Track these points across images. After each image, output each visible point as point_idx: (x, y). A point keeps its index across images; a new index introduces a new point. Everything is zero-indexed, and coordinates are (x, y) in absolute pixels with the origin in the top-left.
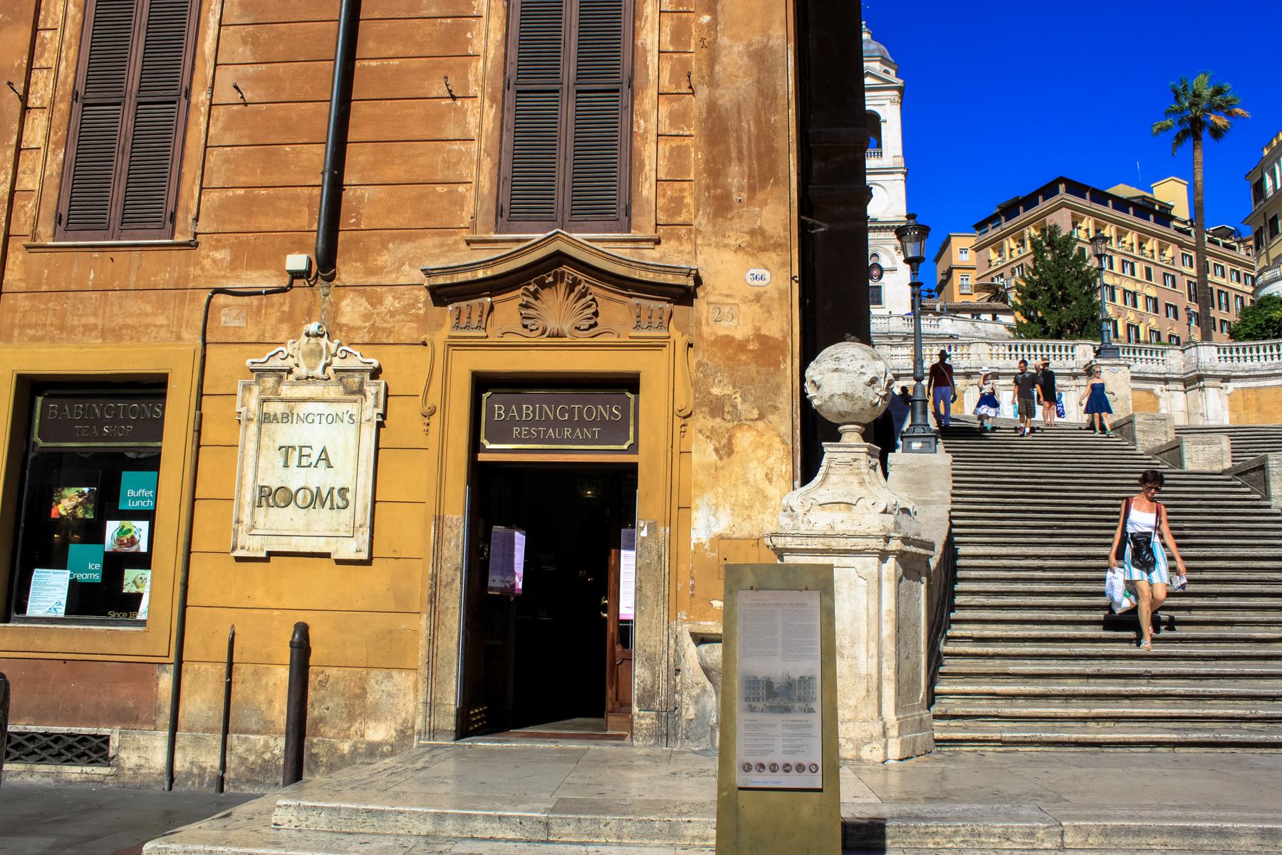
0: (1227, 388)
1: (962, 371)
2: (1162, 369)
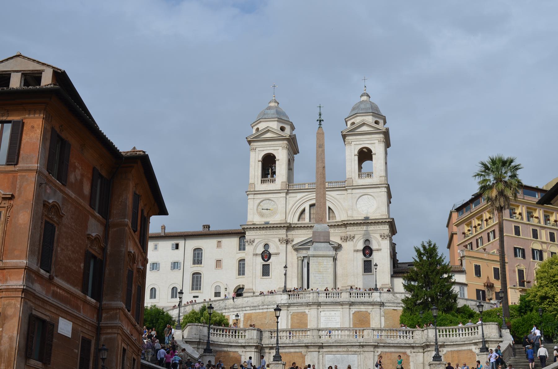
0: (443, 351)
1: (304, 345)
2: (411, 341)
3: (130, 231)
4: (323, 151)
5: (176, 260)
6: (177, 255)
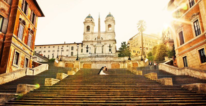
3: (21, 11)
4: (100, 23)
5: (67, 49)
6: (68, 48)
